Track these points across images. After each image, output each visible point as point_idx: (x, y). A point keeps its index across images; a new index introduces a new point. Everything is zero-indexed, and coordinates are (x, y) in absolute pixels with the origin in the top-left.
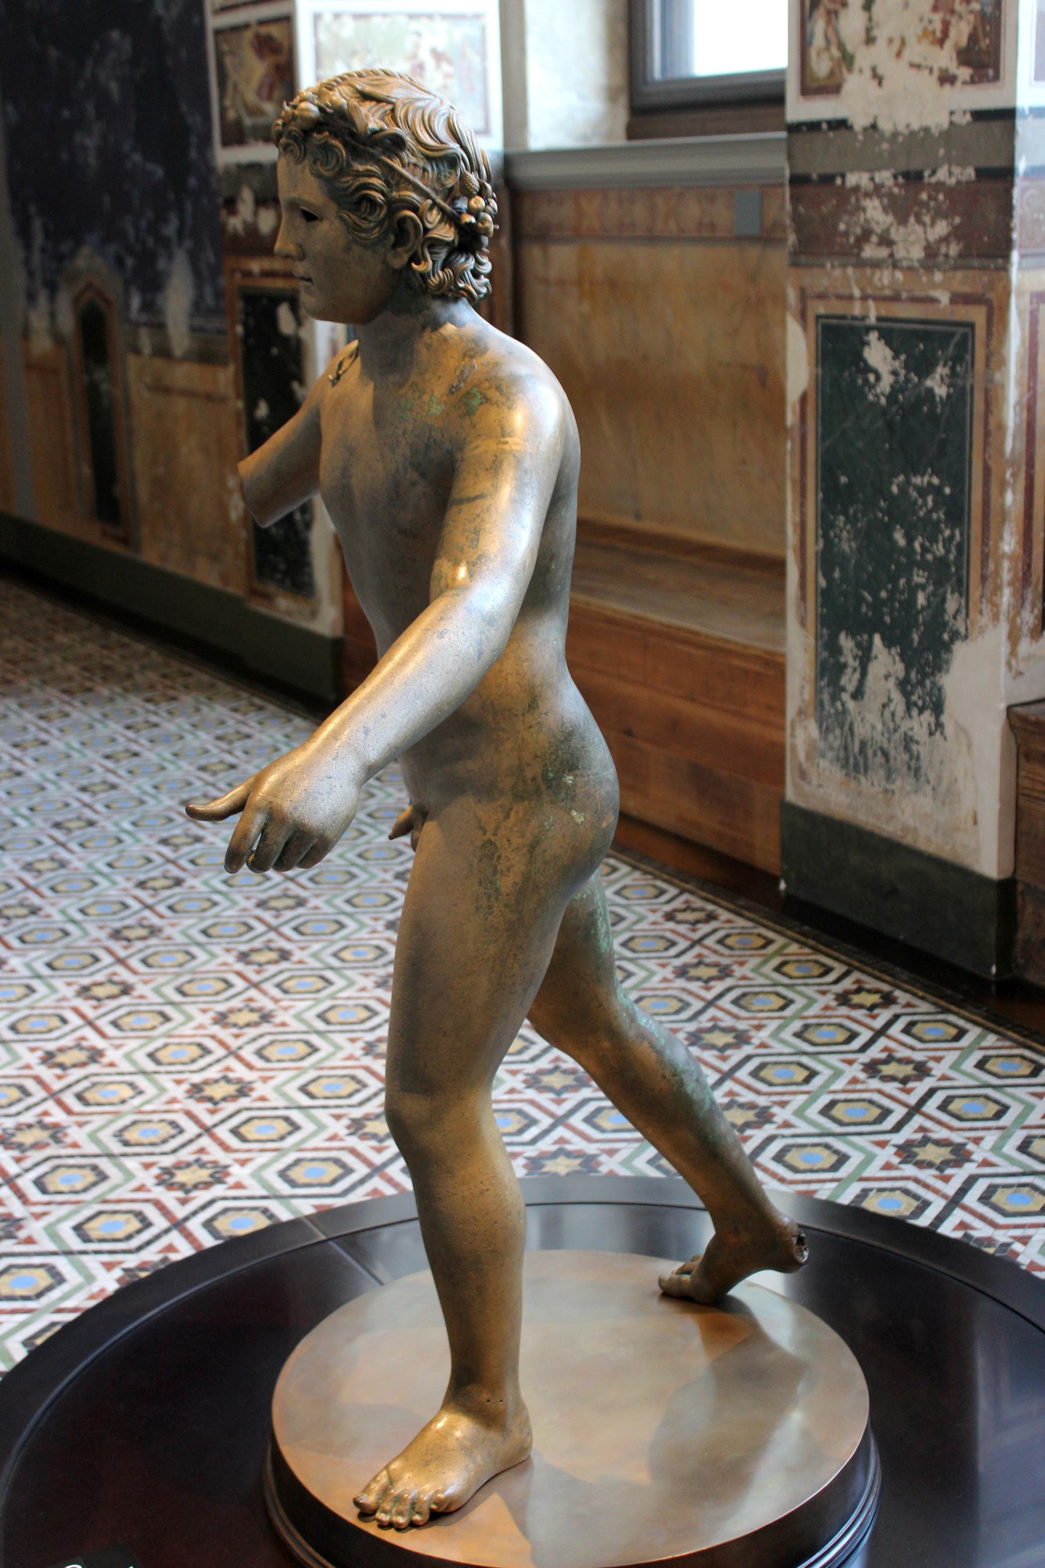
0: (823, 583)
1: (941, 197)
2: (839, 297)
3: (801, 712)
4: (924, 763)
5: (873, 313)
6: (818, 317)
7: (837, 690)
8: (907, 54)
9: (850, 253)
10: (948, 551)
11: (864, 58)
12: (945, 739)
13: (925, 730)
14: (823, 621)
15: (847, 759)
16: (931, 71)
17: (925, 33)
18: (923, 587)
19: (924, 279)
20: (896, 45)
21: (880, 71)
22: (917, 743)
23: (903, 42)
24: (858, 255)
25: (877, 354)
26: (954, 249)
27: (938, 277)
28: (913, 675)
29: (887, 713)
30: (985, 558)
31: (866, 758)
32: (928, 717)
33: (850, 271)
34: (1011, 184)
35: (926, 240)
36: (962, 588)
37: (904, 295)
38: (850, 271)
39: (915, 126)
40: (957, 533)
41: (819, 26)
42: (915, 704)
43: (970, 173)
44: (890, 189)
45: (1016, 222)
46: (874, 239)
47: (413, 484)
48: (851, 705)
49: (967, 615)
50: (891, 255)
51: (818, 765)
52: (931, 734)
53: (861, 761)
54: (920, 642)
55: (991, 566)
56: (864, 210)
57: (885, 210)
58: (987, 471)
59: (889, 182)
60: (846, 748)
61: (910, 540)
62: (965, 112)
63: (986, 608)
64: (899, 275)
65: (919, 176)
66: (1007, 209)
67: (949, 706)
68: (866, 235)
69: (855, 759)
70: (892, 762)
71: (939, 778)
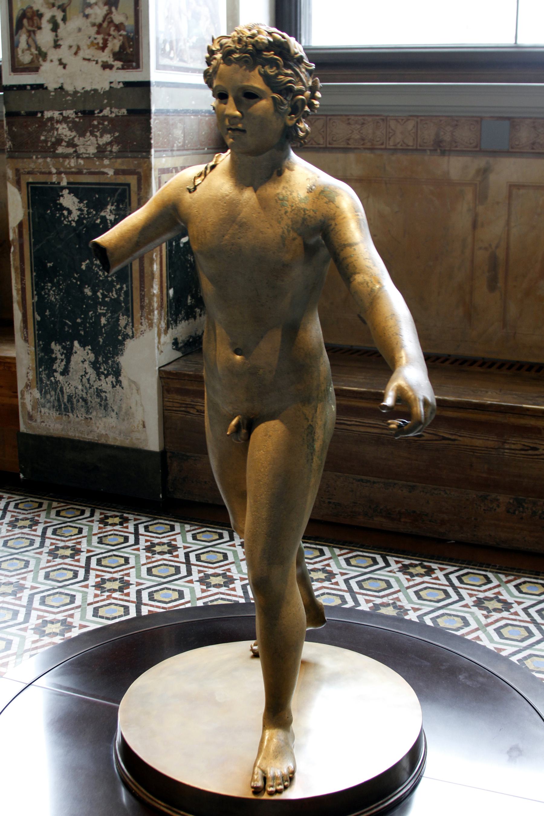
0: (38, 318)
1: (106, 123)
3: (27, 386)
4: (110, 402)
6: (28, 184)
7: (51, 372)
8: (81, 54)
9: (50, 151)
10: (119, 296)
11: (53, 55)
12: (123, 388)
13: (110, 385)
14: (39, 337)
15: (60, 406)
16: (97, 62)
17: (92, 44)
18: (104, 315)
19: (97, 163)
20: (74, 49)
21: (64, 61)
22: (105, 392)
23: (79, 48)
24: (54, 151)
25: (68, 201)
26: (115, 148)
27: (106, 162)
28: (100, 359)
29: (85, 380)
31: (72, 404)
32: (111, 378)
33: (49, 160)
34: (150, 118)
35: (97, 144)
37: (85, 171)
38: (49, 160)
39: (88, 88)
40: (124, 286)
41: (23, 39)
42: (103, 373)
43: (124, 111)
44: (73, 118)
46: (64, 144)
48: (60, 378)
49: (133, 326)
50: (76, 152)
51: (41, 412)
52: (113, 387)
53: (69, 406)
54: (103, 342)
55: (147, 301)
56: (57, 129)
57: (70, 129)
59: (74, 116)
60: (59, 400)
61: (95, 292)
62: (119, 82)
64: (81, 161)
65: (92, 113)
66: (148, 129)
67: (123, 373)
68: (59, 141)
69: (65, 405)
70: (89, 403)
71: (120, 408)
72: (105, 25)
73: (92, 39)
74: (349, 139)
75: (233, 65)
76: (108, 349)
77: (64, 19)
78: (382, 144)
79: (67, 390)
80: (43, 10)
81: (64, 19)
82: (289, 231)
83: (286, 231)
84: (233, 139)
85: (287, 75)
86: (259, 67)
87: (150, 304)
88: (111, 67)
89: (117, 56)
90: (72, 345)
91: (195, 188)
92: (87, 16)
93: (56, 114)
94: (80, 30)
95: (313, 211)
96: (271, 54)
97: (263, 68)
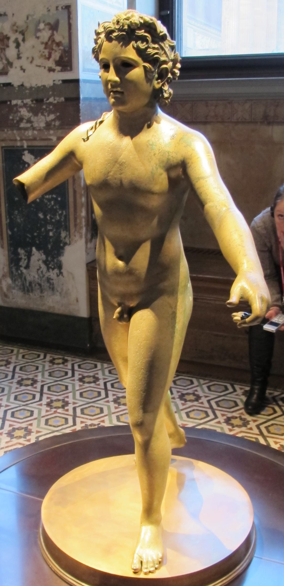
0: (10, 233)
1: (51, 107)
2: (11, 140)
4: (56, 286)
5: (25, 145)
7: (18, 267)
8: (35, 62)
9: (15, 126)
10: (61, 218)
11: (17, 64)
12: (63, 277)
13: (55, 275)
14: (10, 245)
15: (24, 289)
16: (45, 68)
17: (42, 56)
19: (46, 133)
20: (30, 59)
21: (24, 68)
22: (52, 280)
23: (33, 58)
24: (18, 126)
26: (57, 123)
27: (52, 132)
28: (49, 259)
29: (40, 272)
30: (75, 219)
31: (32, 287)
32: (56, 271)
33: (15, 132)
34: (79, 103)
35: (46, 120)
36: (67, 229)
37: (38, 138)
38: (15, 132)
39: (40, 85)
40: (64, 212)
42: (51, 268)
43: (63, 99)
44: (30, 105)
45: (81, 114)
46: (25, 121)
47: (161, 174)
48: (24, 271)
49: (70, 237)
50: (32, 126)
51: (12, 292)
52: (58, 276)
53: (30, 288)
54: (52, 248)
55: (78, 221)
56: (20, 112)
57: (28, 112)
58: (75, 192)
59: (30, 103)
60: (23, 285)
61: (45, 216)
62: (59, 80)
63: (77, 234)
64: (36, 132)
65: (42, 101)
68: (21, 119)
69: (27, 287)
70: (43, 287)
71: (62, 289)
72: (50, 43)
73: (41, 52)
74: (207, 116)
75: (114, 42)
76: (53, 252)
77: (24, 40)
78: (229, 118)
79: (29, 278)
80: (10, 34)
81: (24, 40)
82: (157, 169)
83: (154, 168)
85: (154, 48)
86: (133, 43)
87: (81, 223)
88: (53, 70)
89: (58, 63)
90: (31, 251)
91: (88, 138)
92: (38, 38)
93: (19, 102)
94: (33, 47)
95: (175, 153)
96: (141, 32)
97: (136, 42)
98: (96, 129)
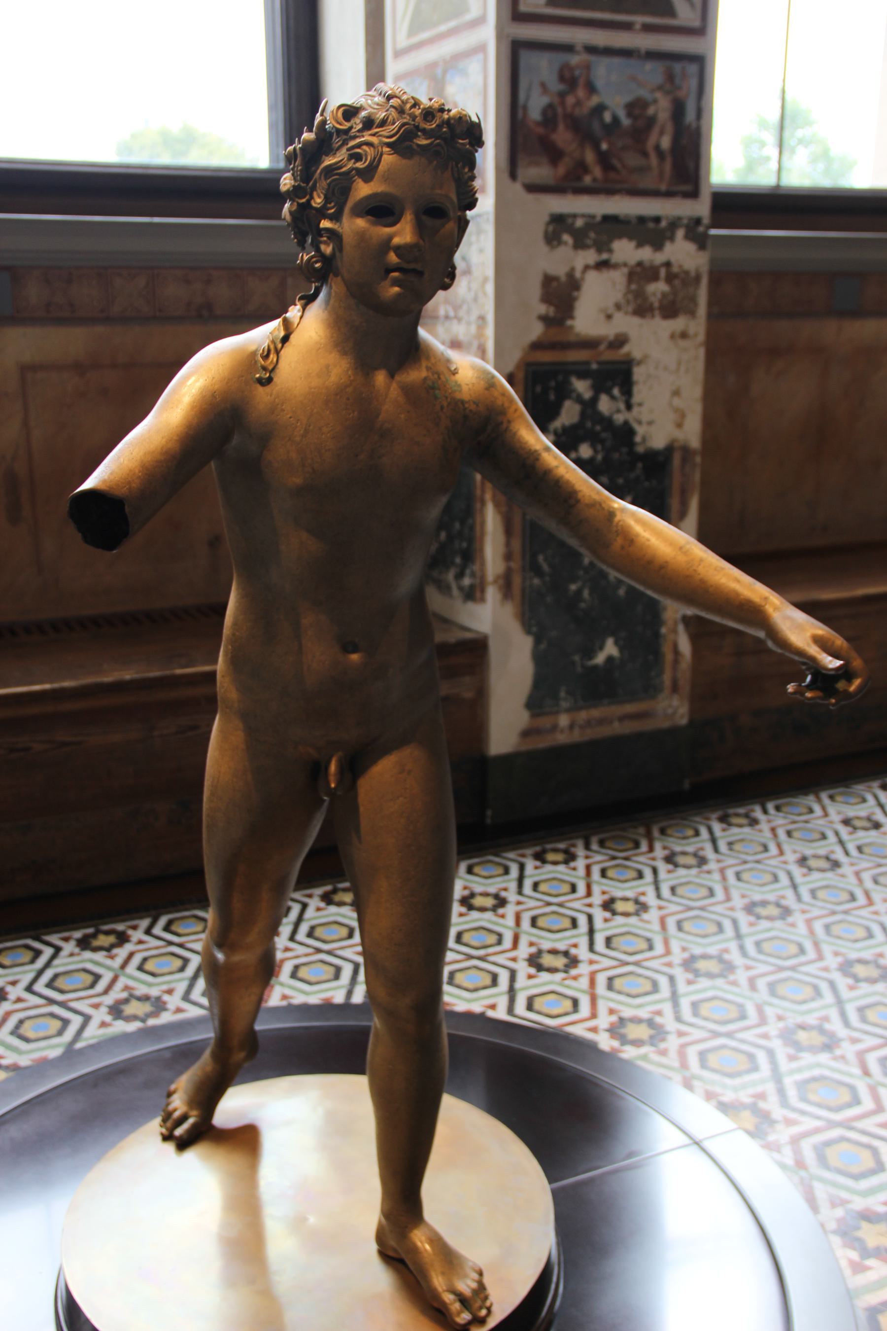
84: (398, 286)
98: (278, 352)
